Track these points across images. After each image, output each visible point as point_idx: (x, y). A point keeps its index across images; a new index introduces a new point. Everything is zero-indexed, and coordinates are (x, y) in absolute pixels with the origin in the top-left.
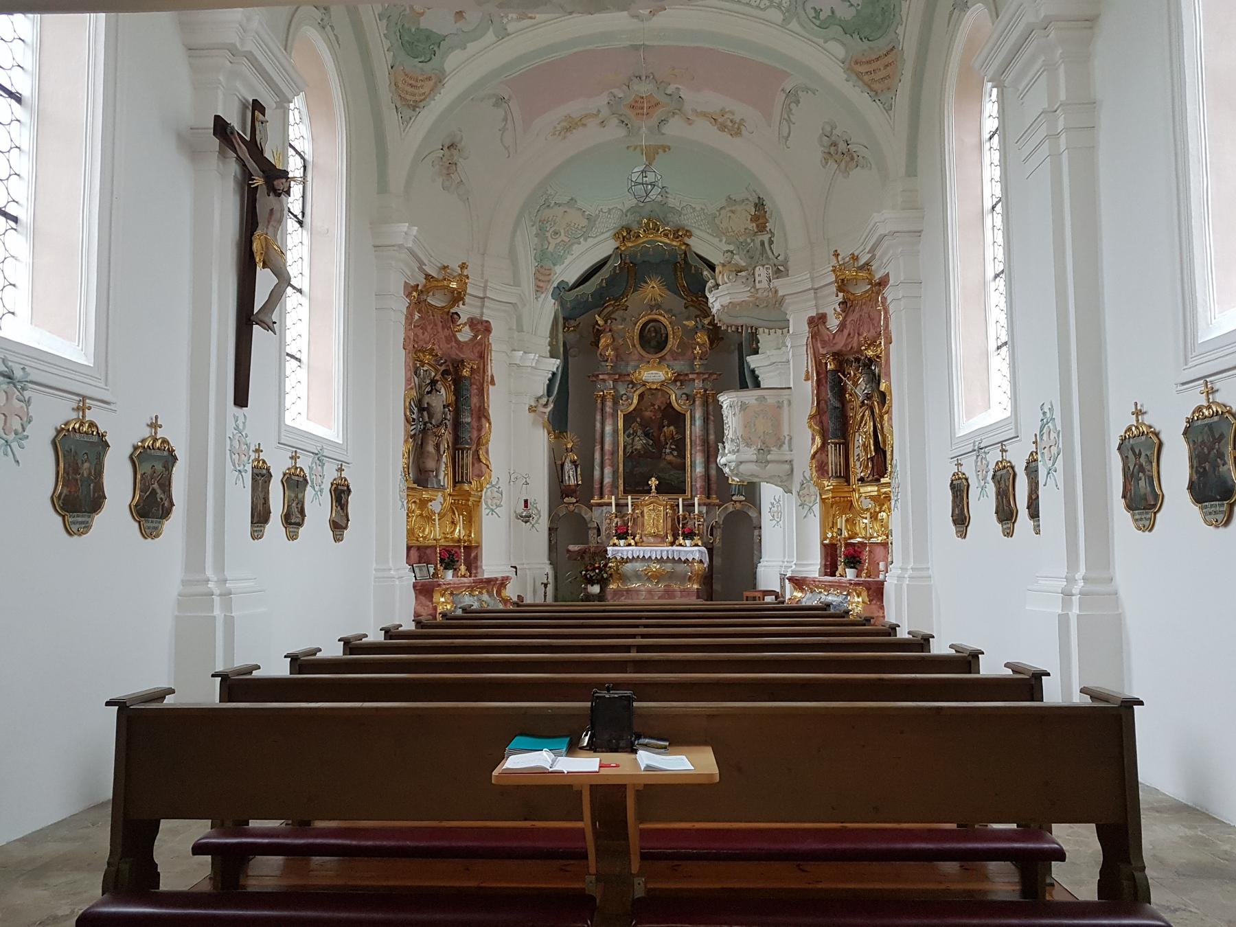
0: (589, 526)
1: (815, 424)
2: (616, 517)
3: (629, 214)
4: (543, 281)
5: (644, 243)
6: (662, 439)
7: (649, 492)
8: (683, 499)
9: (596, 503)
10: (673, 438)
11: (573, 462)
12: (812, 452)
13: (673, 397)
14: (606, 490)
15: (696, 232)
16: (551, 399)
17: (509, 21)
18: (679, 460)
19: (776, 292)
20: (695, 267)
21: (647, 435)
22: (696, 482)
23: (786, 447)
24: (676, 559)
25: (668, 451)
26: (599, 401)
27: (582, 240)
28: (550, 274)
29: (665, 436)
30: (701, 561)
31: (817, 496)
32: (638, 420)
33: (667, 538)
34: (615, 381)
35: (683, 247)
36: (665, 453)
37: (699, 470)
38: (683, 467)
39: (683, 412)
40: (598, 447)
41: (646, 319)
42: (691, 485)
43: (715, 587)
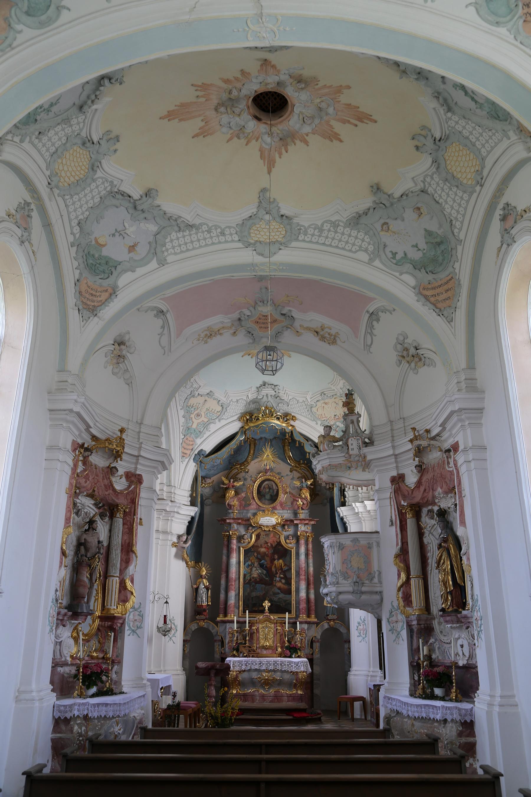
1: (400, 562)
4: (187, 449)
5: (261, 424)
6: (273, 569)
7: (263, 611)
10: (282, 569)
12: (399, 585)
16: (189, 537)
17: (169, 255)
18: (286, 587)
19: (365, 457)
20: (299, 441)
21: (261, 566)
22: (299, 604)
23: (376, 580)
25: (278, 579)
29: (275, 567)
31: (404, 622)
32: (255, 554)
35: (290, 428)
36: (276, 580)
38: (289, 592)
40: (223, 576)
41: (263, 478)
43: (315, 691)
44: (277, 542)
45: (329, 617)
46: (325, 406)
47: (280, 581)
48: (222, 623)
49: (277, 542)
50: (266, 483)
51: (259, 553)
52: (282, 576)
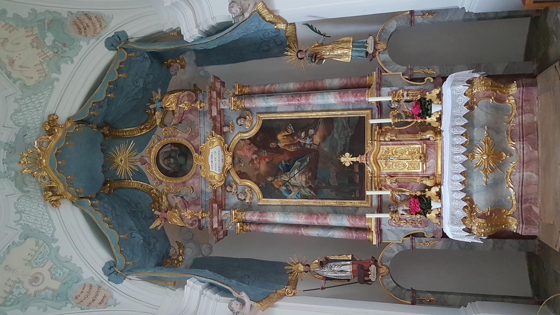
0: (409, 248)
2: (396, 212)
6: (292, 149)
7: (362, 167)
8: (372, 119)
9: (377, 238)
10: (292, 135)
11: (322, 264)
13: (247, 136)
14: (359, 223)
15: (50, 109)
18: (321, 127)
21: (288, 169)
22: (349, 103)
24: (466, 121)
26: (248, 228)
27: (54, 245)
28: (91, 286)
29: (289, 146)
30: (470, 82)
32: (270, 179)
33: (429, 139)
34: (222, 207)
36: (311, 145)
37: (331, 99)
38: (329, 121)
39: (261, 122)
40: (304, 232)
42: (353, 110)
43: (500, 73)
44: (250, 144)
45: (370, 50)
46: (17, 63)
47: (311, 137)
48: (381, 237)
49: (250, 144)
50: (161, 162)
51: (268, 174)
52: (303, 135)
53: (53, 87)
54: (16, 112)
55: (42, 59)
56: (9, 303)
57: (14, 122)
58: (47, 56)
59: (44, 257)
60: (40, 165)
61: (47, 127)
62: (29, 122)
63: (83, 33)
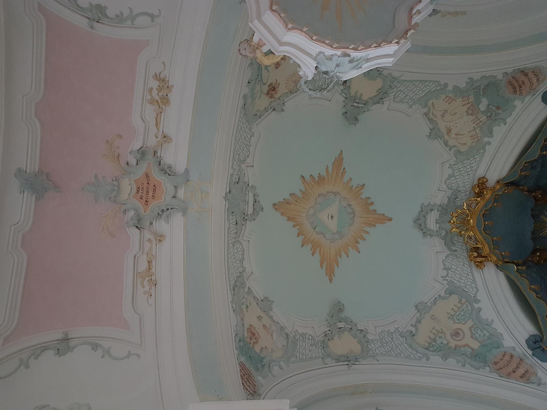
3: (454, 248)
15: (480, 173)
27: (476, 306)
28: (512, 356)
46: (454, 131)
53: (485, 151)
54: (450, 176)
55: (476, 125)
56: (431, 349)
57: (447, 186)
58: (481, 122)
59: (466, 315)
60: (467, 225)
61: (477, 189)
62: (460, 186)
63: (518, 92)
